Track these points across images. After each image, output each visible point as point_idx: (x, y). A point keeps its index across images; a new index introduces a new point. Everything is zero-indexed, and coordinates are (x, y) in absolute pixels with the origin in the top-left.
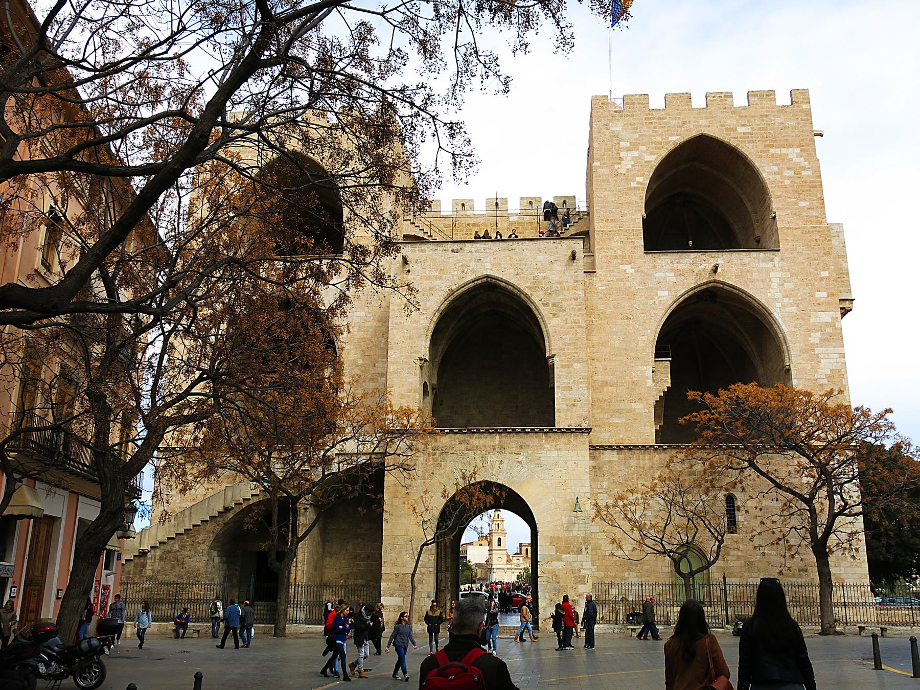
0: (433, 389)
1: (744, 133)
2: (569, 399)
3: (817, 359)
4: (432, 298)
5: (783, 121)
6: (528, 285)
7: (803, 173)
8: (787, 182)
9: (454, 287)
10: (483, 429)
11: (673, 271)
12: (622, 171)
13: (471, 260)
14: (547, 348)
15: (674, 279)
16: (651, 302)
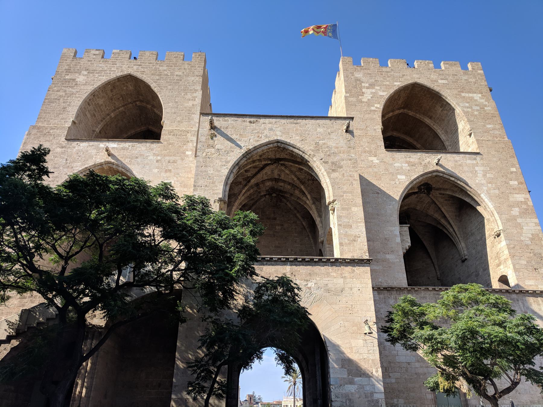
4: (231, 154)
6: (312, 148)
7: (486, 108)
8: (476, 113)
9: (251, 147)
12: (365, 100)
13: (265, 129)
15: (408, 168)
16: (393, 183)
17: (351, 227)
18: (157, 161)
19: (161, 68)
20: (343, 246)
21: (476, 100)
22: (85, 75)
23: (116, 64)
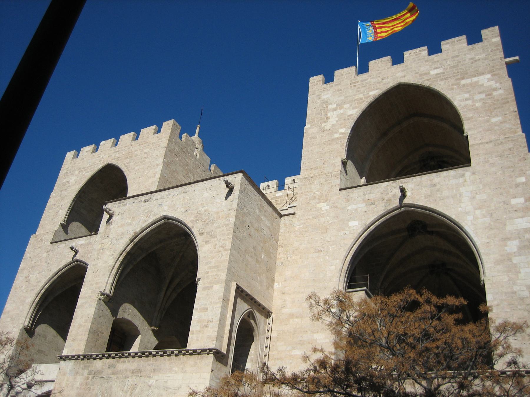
1: (437, 74)
3: (514, 269)
6: (192, 218)
7: (495, 93)
8: (478, 104)
9: (138, 230)
11: (364, 201)
15: (365, 209)
16: (342, 233)
17: (207, 309)
19: (133, 149)
20: (193, 334)
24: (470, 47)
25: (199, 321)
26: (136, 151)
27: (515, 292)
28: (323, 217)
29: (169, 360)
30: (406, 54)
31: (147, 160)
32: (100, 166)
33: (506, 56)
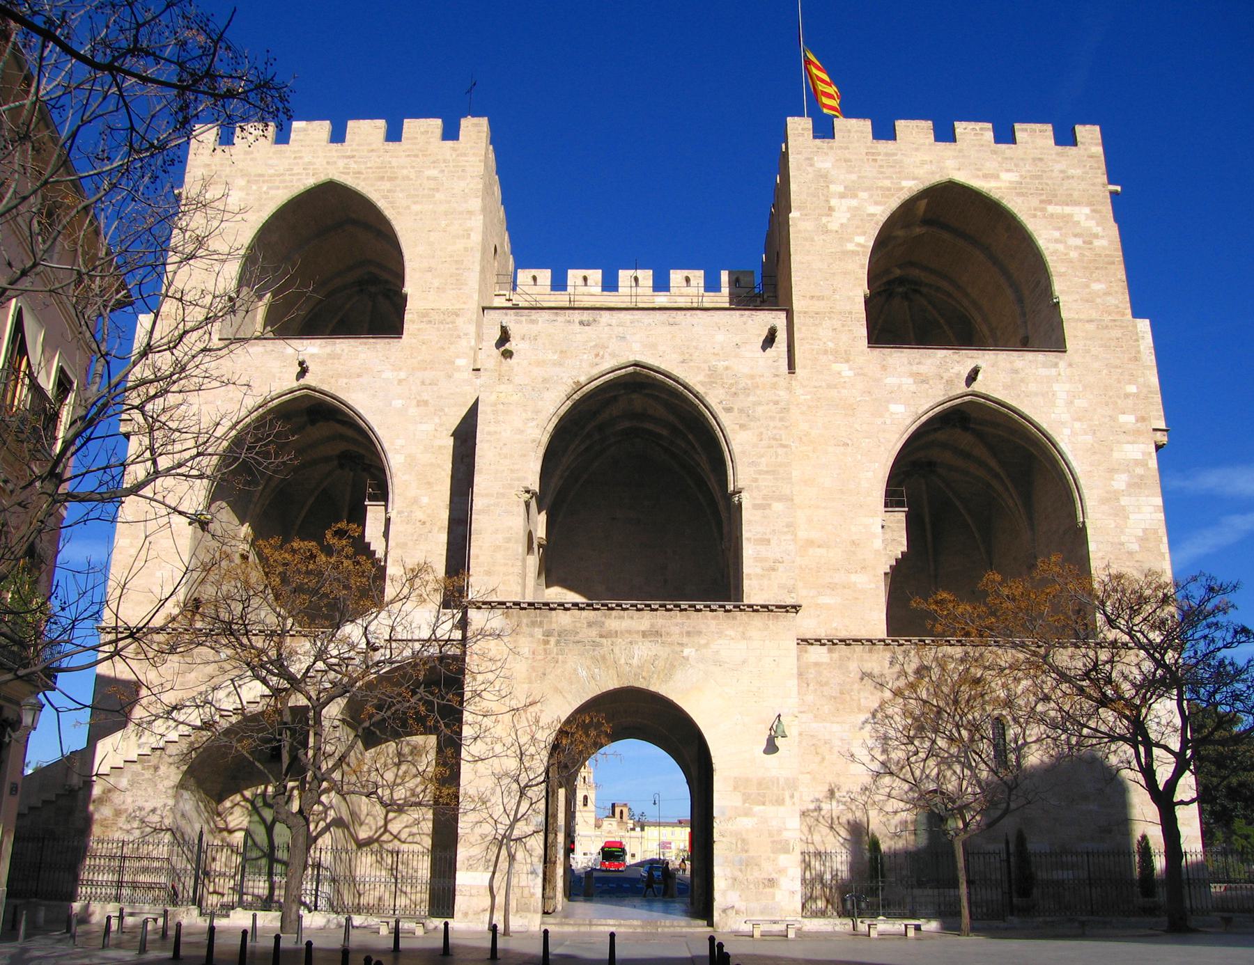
0: (540, 546)
2: (765, 560)
3: (1121, 514)
4: (547, 395)
5: (1063, 168)
6: (701, 378)
7: (1097, 243)
8: (1073, 255)
9: (583, 379)
10: (626, 604)
11: (912, 375)
12: (834, 226)
14: (731, 478)
15: (913, 388)
16: (879, 421)
17: (769, 541)
18: (400, 381)
21: (1079, 223)
22: (241, 189)
23: (301, 158)
24: (1059, 148)
25: (757, 559)
26: (403, 168)
27: (1123, 544)
28: (844, 387)
29: (714, 618)
30: (960, 127)
31: (437, 195)
32: (310, 182)
33: (1110, 182)
